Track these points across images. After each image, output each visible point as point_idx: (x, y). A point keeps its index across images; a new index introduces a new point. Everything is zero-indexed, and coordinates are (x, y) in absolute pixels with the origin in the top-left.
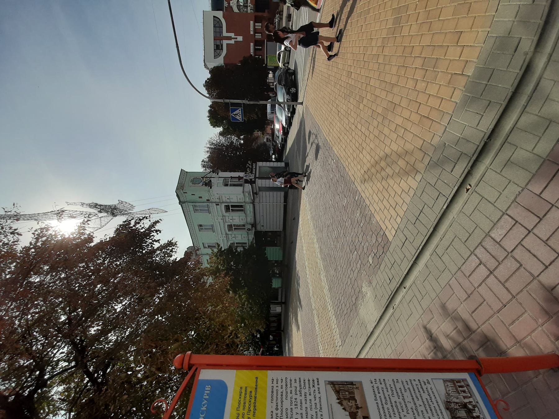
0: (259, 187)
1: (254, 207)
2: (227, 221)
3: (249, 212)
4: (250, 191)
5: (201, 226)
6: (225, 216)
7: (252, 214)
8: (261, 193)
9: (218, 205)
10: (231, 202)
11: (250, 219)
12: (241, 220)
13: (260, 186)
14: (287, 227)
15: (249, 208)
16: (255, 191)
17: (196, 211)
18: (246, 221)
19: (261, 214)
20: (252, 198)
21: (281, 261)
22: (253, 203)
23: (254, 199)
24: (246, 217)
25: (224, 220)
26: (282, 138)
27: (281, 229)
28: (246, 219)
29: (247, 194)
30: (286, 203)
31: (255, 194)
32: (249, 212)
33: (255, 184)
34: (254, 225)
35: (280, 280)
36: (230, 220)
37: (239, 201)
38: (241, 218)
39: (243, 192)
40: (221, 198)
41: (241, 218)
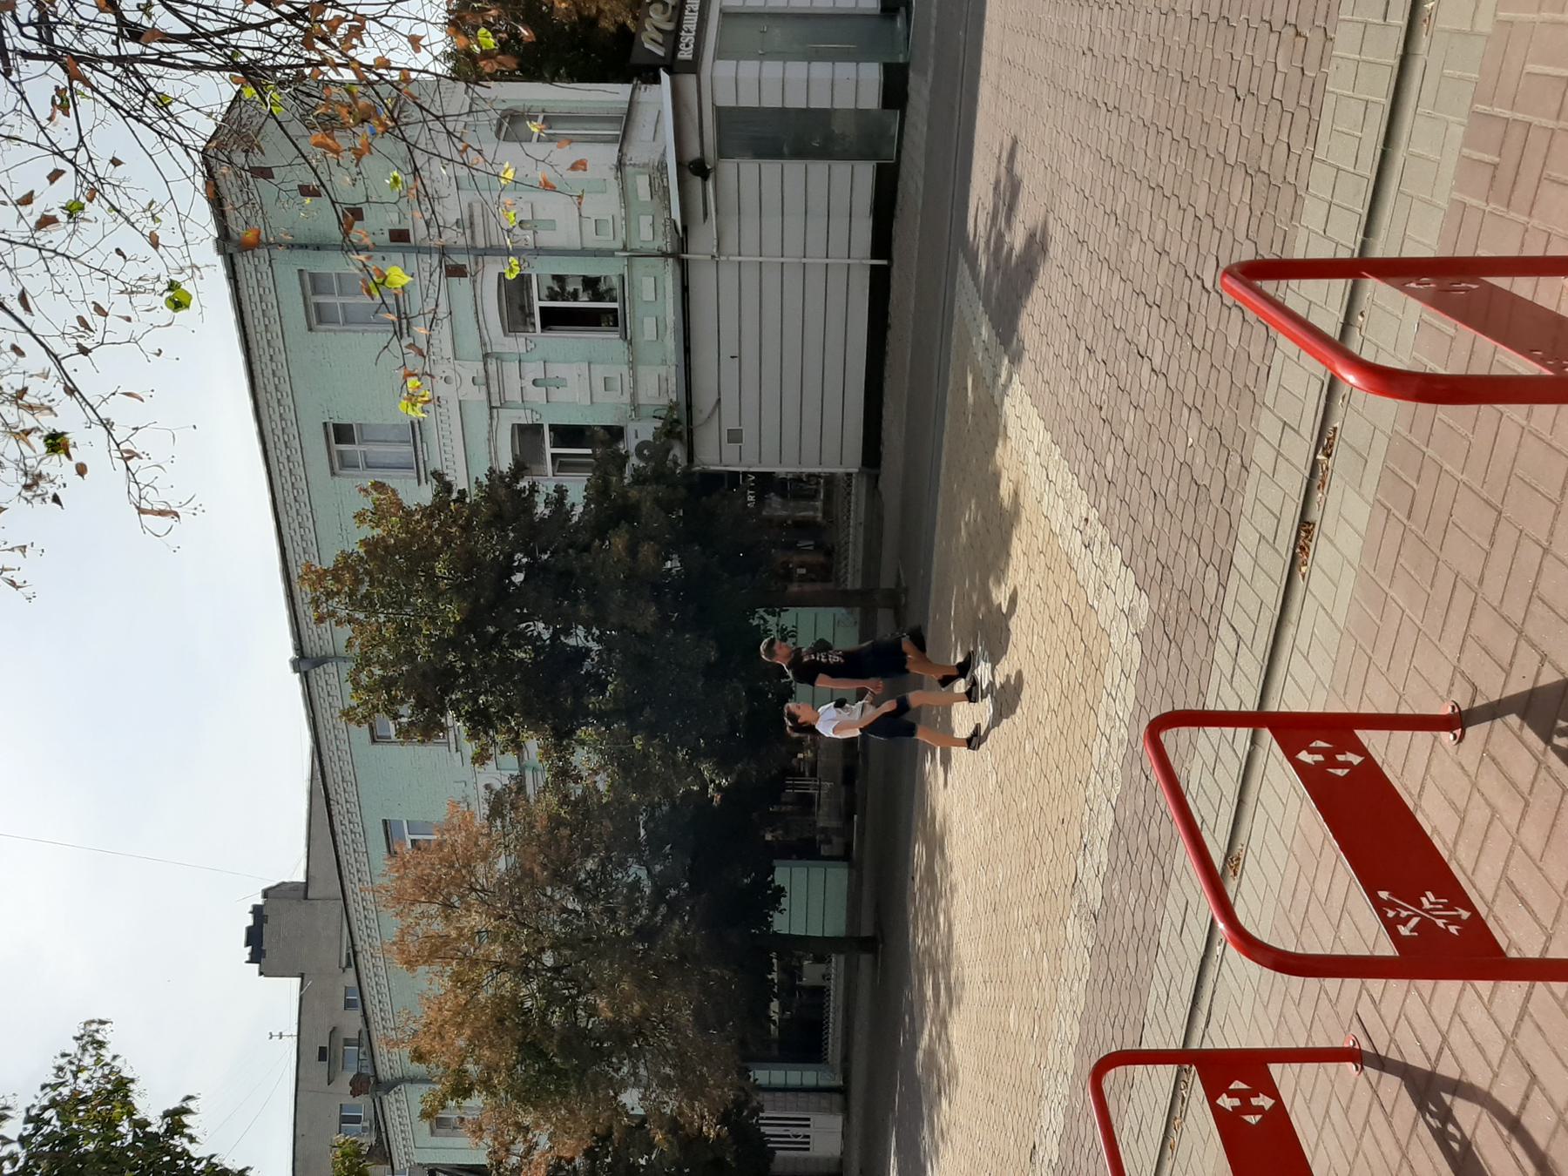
0: (720, 112)
1: (685, 289)
2: (513, 395)
4: (662, 167)
5: (342, 433)
6: (499, 358)
7: (671, 343)
8: (728, 168)
9: (457, 271)
10: (539, 251)
12: (599, 384)
13: (726, 100)
14: (886, 450)
16: (693, 152)
17: (318, 317)
18: (634, 395)
19: (729, 348)
20: (676, 215)
22: (679, 253)
23: (685, 229)
24: (632, 365)
25: (494, 389)
27: (850, 461)
28: (635, 382)
29: (642, 183)
30: (888, 256)
31: (695, 169)
33: (694, 76)
34: (682, 428)
35: (837, 877)
36: (528, 384)
37: (592, 242)
38: (599, 372)
39: (620, 165)
40: (478, 220)
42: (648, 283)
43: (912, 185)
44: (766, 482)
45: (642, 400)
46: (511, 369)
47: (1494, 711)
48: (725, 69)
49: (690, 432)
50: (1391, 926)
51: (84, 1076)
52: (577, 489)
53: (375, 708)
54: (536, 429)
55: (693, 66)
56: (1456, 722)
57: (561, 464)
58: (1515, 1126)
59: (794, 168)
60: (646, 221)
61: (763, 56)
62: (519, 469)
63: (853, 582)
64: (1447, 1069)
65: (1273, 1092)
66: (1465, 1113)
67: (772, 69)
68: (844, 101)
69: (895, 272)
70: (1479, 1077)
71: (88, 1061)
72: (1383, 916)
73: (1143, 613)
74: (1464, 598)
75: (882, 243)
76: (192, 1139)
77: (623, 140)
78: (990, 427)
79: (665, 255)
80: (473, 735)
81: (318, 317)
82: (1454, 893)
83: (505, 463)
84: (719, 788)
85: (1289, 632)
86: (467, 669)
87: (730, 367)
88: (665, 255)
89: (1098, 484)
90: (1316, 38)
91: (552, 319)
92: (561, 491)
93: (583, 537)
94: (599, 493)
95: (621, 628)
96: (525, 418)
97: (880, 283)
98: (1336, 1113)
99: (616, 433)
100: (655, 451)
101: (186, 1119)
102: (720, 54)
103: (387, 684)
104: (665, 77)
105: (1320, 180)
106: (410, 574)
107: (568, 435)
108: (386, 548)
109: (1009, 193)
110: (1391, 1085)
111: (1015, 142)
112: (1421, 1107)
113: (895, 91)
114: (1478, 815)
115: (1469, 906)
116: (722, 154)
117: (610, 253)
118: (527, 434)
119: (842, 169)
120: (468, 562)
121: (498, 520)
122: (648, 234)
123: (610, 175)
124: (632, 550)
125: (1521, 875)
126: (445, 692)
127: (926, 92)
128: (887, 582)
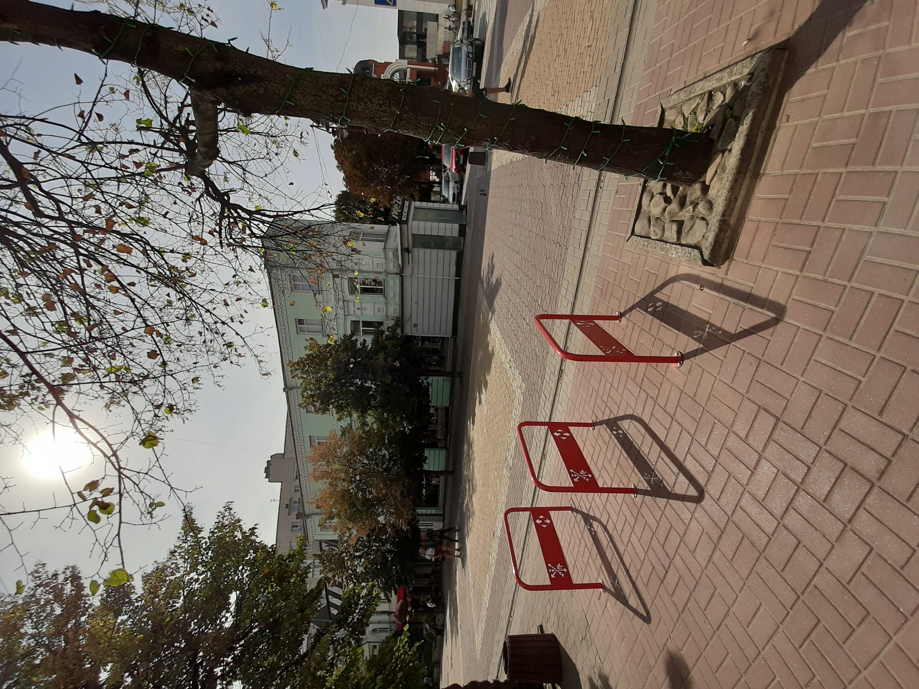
0: (413, 235)
3: (392, 294)
4: (397, 250)
5: (301, 322)
6: (348, 301)
7: (398, 299)
8: (415, 250)
9: (337, 276)
11: (393, 310)
12: (376, 310)
13: (415, 232)
15: (393, 285)
16: (406, 246)
18: (386, 313)
19: (415, 300)
20: (400, 262)
21: (447, 409)
22: (401, 273)
24: (386, 304)
26: (454, 194)
29: (391, 254)
30: (460, 277)
31: (406, 250)
32: (392, 294)
35: (442, 453)
37: (376, 269)
38: (377, 306)
39: (385, 248)
41: (377, 306)
42: (392, 281)
43: (467, 258)
44: (424, 339)
45: (389, 314)
46: (351, 305)
47: (601, 423)
48: (415, 223)
49: (403, 325)
50: (572, 479)
51: (225, 518)
52: (369, 339)
53: (309, 404)
54: (358, 322)
55: (406, 222)
56: (593, 425)
57: (365, 332)
58: (605, 528)
59: (434, 251)
60: (391, 264)
61: (426, 221)
62: (353, 334)
63: (449, 369)
64: (591, 513)
65: (550, 519)
66: (595, 524)
67: (429, 224)
68: (448, 234)
69: (462, 282)
70: (598, 516)
71: (227, 514)
72: (571, 476)
73: (523, 387)
74: (594, 394)
75: (458, 273)
76: (257, 537)
77: (386, 241)
78: (487, 331)
79: (397, 274)
80: (337, 413)
81: (295, 288)
82: (589, 471)
83: (349, 332)
84: (408, 429)
85: (557, 397)
86: (336, 393)
87: (414, 306)
88: (397, 274)
89: (513, 351)
90: (564, 247)
91: (365, 291)
92: (365, 341)
93: (371, 355)
94: (375, 342)
95: (381, 382)
96: (355, 319)
97: (458, 284)
98: (567, 524)
99: (381, 323)
100: (393, 329)
101: (255, 531)
102: (414, 219)
103: (312, 396)
104: (398, 225)
105: (565, 283)
106: (319, 364)
107: (366, 324)
108: (313, 357)
109: (492, 268)
110: (579, 516)
111: (493, 255)
112: (586, 523)
113: (462, 231)
114: (598, 448)
115: (591, 473)
116: (414, 247)
117: (381, 273)
118: (355, 324)
119: (447, 252)
120: (337, 361)
121: (346, 349)
122: (392, 268)
123: (382, 251)
124: (385, 359)
125: (606, 464)
126: (330, 399)
127: (471, 234)
128: (458, 370)
